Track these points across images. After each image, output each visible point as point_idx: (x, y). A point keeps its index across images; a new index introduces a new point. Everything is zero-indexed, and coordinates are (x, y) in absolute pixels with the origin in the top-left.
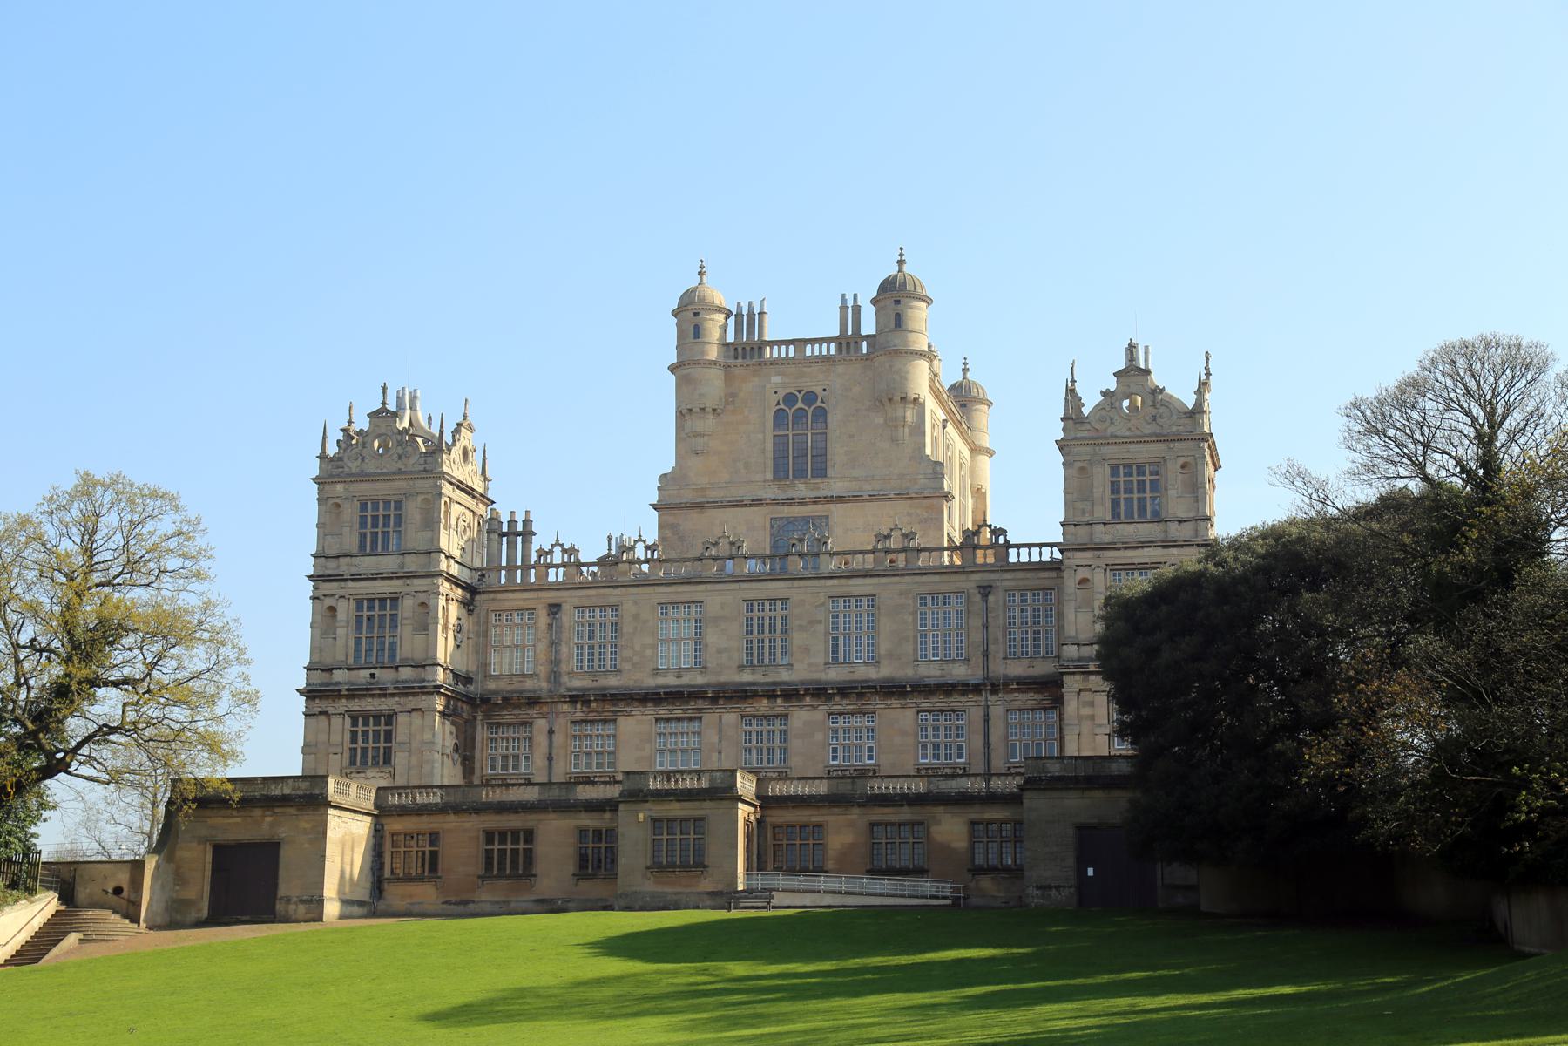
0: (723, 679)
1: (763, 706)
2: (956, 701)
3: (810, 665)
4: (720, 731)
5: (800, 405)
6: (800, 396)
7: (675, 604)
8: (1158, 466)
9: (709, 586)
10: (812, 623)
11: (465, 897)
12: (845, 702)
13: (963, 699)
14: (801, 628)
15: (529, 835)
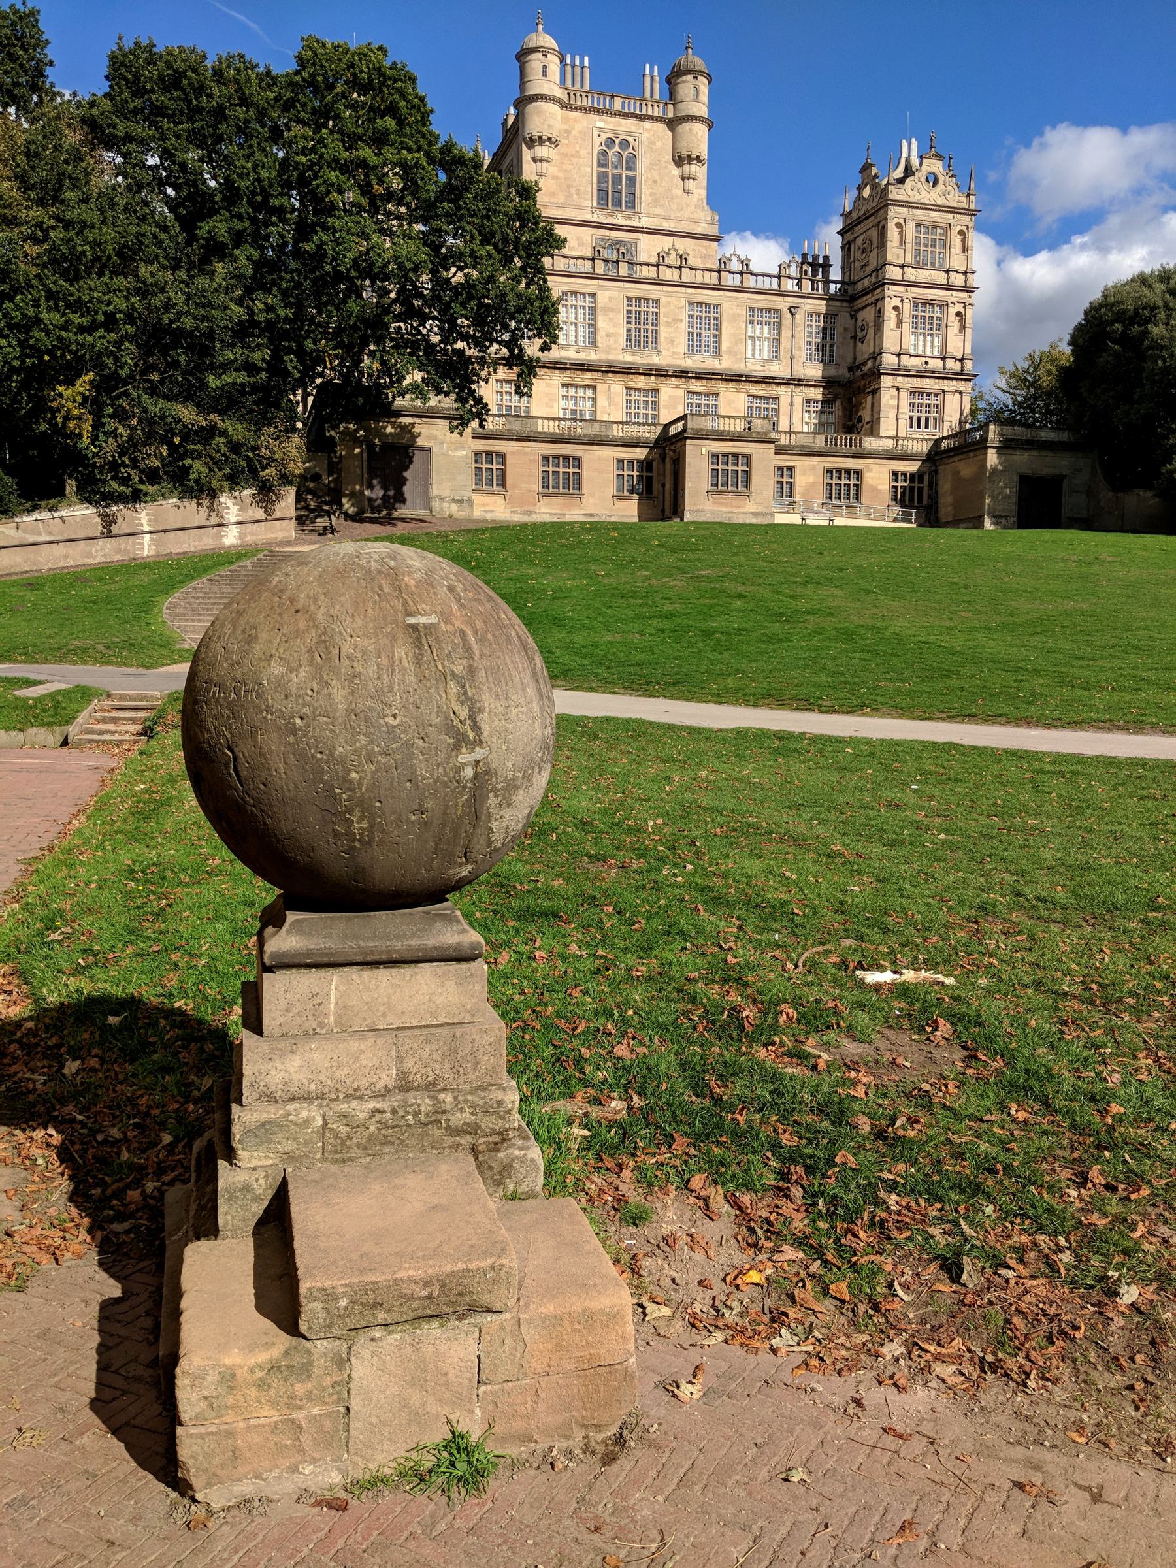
0: (611, 357)
1: (640, 381)
2: (772, 390)
3: (674, 353)
4: (609, 398)
5: (617, 148)
6: (617, 141)
9: (601, 282)
10: (676, 320)
11: (527, 508)
12: (699, 383)
13: (778, 389)
14: (668, 324)
15: (578, 459)
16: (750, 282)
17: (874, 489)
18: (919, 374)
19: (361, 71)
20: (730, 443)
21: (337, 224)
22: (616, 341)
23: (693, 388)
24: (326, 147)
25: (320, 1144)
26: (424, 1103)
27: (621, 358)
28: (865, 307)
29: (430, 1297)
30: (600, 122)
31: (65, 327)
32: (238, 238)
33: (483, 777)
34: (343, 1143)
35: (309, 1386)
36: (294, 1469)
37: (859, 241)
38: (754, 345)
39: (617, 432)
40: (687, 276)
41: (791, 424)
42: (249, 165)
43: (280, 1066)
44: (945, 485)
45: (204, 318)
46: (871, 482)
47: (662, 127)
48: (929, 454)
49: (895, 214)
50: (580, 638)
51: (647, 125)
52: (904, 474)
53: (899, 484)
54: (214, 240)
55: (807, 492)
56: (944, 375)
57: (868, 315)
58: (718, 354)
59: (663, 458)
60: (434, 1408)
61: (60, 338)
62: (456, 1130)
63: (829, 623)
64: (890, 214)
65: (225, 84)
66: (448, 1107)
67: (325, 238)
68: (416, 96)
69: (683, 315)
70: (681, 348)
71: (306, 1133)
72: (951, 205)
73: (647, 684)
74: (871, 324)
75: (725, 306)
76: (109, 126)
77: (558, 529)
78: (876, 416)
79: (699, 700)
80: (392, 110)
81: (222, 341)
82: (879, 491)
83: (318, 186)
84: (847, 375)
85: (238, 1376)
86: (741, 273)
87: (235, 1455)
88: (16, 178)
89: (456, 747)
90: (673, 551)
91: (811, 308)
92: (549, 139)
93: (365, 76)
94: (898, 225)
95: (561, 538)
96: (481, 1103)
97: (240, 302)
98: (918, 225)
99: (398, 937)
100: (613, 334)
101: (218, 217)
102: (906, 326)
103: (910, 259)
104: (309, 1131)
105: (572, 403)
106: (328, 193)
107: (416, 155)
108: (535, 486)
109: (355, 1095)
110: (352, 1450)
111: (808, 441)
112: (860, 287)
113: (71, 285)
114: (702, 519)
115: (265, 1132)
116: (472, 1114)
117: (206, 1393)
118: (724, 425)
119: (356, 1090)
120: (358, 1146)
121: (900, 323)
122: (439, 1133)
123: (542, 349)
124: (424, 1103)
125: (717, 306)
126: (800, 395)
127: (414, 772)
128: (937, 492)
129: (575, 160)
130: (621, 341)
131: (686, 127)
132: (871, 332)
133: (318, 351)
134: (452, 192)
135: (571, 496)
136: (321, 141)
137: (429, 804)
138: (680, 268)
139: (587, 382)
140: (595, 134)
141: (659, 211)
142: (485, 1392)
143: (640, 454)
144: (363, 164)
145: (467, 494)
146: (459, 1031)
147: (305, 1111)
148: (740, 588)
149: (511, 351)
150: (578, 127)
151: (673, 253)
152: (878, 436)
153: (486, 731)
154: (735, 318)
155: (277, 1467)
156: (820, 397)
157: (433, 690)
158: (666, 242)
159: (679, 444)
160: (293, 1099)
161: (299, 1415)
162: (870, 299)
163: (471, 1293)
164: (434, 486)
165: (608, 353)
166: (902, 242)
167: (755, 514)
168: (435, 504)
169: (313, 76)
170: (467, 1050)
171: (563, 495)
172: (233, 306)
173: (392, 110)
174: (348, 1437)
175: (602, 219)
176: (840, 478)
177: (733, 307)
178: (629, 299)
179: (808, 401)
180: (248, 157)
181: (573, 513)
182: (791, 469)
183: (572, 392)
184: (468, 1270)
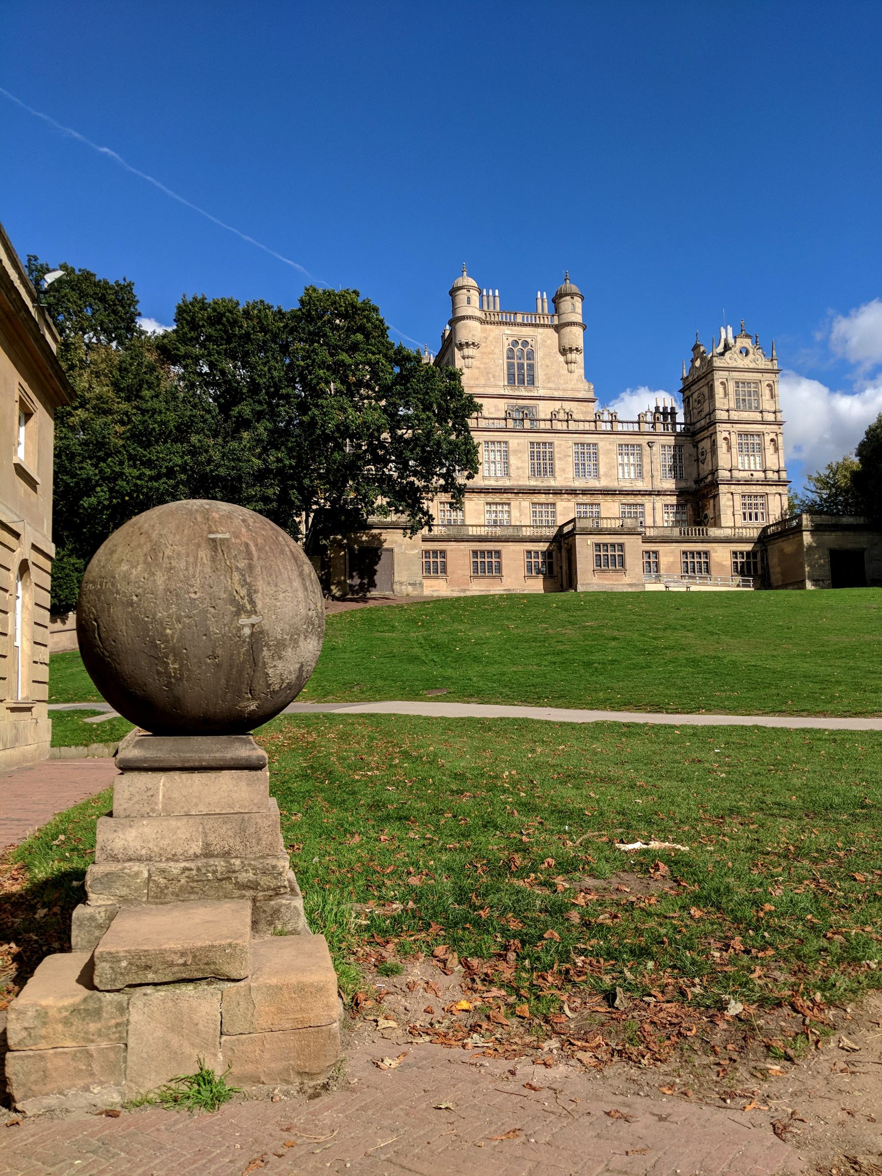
0: (520, 483)
1: (542, 498)
2: (639, 499)
3: (565, 478)
4: (520, 510)
5: (520, 347)
6: (520, 342)
7: (493, 442)
8: (758, 383)
10: (566, 456)
12: (585, 497)
13: (643, 498)
14: (560, 459)
15: (498, 553)
16: (619, 427)
17: (721, 566)
18: (747, 483)
19: (341, 306)
20: (608, 536)
21: (325, 403)
22: (524, 472)
23: (580, 501)
24: (317, 354)
25: (146, 891)
26: (220, 864)
27: (528, 483)
28: (703, 439)
29: (185, 964)
30: (507, 330)
31: (139, 478)
32: (259, 416)
33: (258, 637)
34: (162, 892)
35: (99, 1025)
36: (86, 1089)
37: (695, 396)
38: (623, 469)
39: (527, 532)
40: (573, 426)
41: (654, 522)
42: (266, 369)
43: (122, 836)
44: (774, 560)
45: (233, 468)
46: (717, 559)
47: (551, 332)
48: (759, 538)
49: (719, 377)
50: (493, 670)
51: (541, 330)
52: (742, 553)
53: (739, 560)
54: (242, 417)
55: (669, 569)
56: (766, 483)
57: (706, 444)
58: (597, 476)
59: (560, 549)
60: (188, 1050)
61: (136, 485)
62: (243, 886)
63: (682, 655)
64: (716, 377)
65: (251, 319)
66: (237, 868)
67: (316, 412)
68: (377, 319)
69: (571, 452)
70: (570, 472)
71: (136, 883)
72: (760, 367)
73: (539, 698)
74: (709, 451)
75: (601, 444)
76: (174, 349)
77: (483, 600)
78: (717, 514)
79: (576, 708)
80: (361, 329)
81: (247, 483)
82: (724, 566)
83: (312, 379)
84: (694, 486)
85: (50, 1014)
86: (611, 422)
87: (45, 1075)
88: (112, 384)
89: (238, 614)
90: (567, 610)
91: (664, 442)
92: (473, 343)
93: (343, 309)
94: (722, 383)
95: (484, 605)
96: (260, 866)
97: (259, 458)
98: (737, 383)
99: (207, 752)
100: (521, 468)
101: (245, 402)
102: (734, 450)
103: (732, 405)
104: (139, 881)
105: (494, 515)
106: (318, 383)
107: (377, 356)
108: (468, 571)
109: (174, 858)
110: (129, 1078)
111: (667, 532)
112: (698, 426)
113: (145, 450)
114: (591, 590)
115: (109, 879)
116: (254, 874)
117: (26, 1025)
118: (604, 524)
119: (174, 855)
120: (173, 893)
121: (729, 448)
122: (230, 887)
123: (468, 478)
124: (220, 864)
125: (595, 445)
126: (660, 502)
127: (208, 629)
128: (767, 564)
129: (491, 356)
130: (528, 472)
131: (568, 329)
132: (709, 456)
133: (313, 486)
134: (403, 379)
135: (494, 577)
136: (314, 351)
137: (219, 652)
138: (567, 421)
139: (504, 501)
140: (505, 338)
141: (551, 385)
142: (225, 1041)
143: (543, 547)
144: (342, 363)
145: (419, 579)
146: (246, 816)
147: (136, 867)
148: (616, 633)
149: (446, 481)
150: (493, 335)
151: (562, 412)
152: (721, 527)
153: (259, 605)
154: (608, 452)
155: (74, 1086)
156: (675, 502)
157: (222, 577)
158: (557, 405)
159: (571, 539)
160: (130, 860)
161: (92, 1047)
162: (706, 433)
163: (214, 963)
164: (396, 575)
165: (518, 480)
166: (726, 394)
167: (630, 585)
168: (396, 587)
169: (309, 311)
170: (253, 830)
171: (488, 577)
172: (254, 459)
173: (361, 329)
174: (126, 1067)
175: (511, 393)
176: (693, 558)
177: (607, 445)
178: (532, 443)
179: (667, 506)
180: (265, 364)
181: (496, 588)
182: (656, 553)
183: (494, 508)
184: (213, 946)
